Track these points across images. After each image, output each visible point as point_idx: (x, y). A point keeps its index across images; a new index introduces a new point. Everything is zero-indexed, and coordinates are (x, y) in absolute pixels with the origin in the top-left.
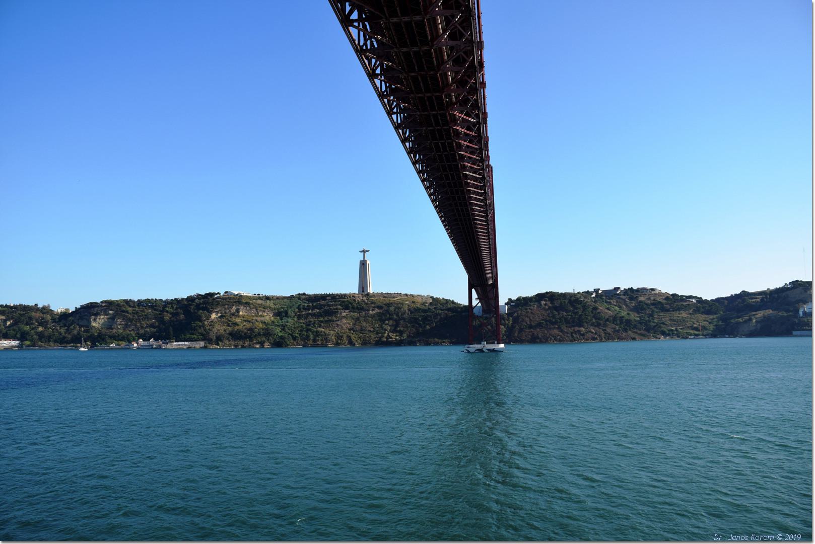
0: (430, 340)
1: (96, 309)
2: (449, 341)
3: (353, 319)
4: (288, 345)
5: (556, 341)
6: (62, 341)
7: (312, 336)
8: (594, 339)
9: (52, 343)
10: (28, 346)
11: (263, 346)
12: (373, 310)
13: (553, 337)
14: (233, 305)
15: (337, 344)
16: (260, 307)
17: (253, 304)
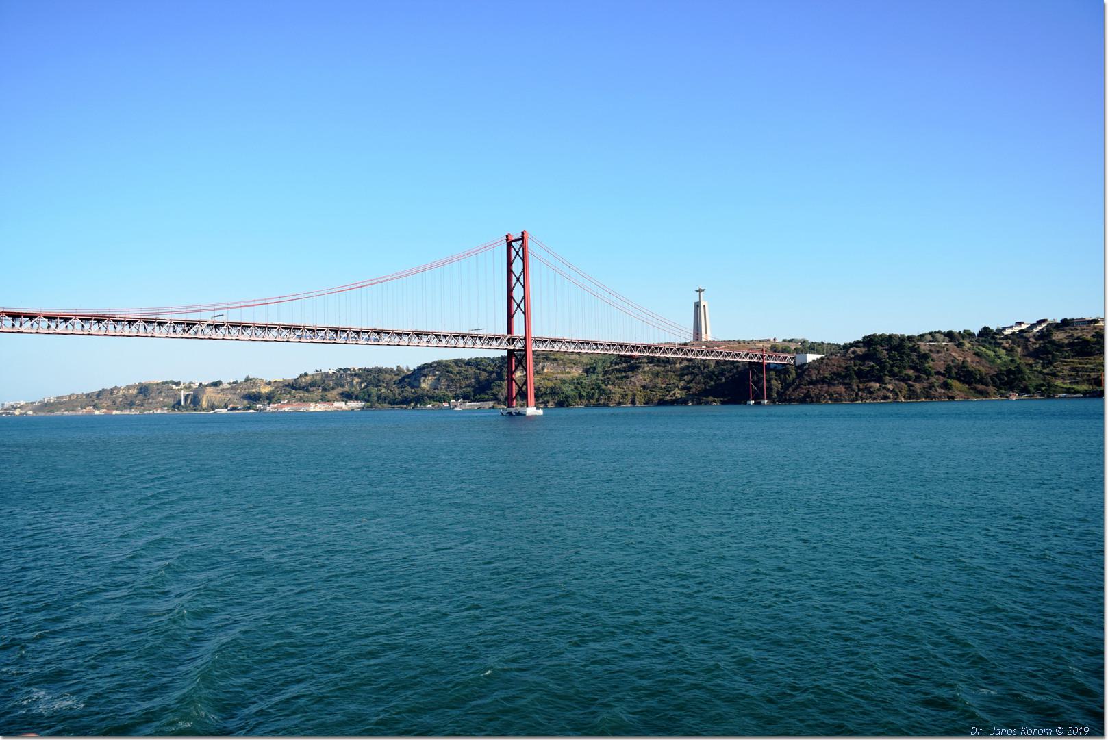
0: (704, 398)
1: (426, 370)
2: (722, 399)
3: (652, 374)
4: (570, 405)
5: (831, 399)
6: (393, 402)
7: (596, 396)
8: (885, 398)
9: (385, 405)
10: (368, 407)
11: (547, 406)
12: (680, 363)
13: (829, 395)
14: (540, 362)
15: (619, 404)
16: (571, 363)
17: (562, 360)
